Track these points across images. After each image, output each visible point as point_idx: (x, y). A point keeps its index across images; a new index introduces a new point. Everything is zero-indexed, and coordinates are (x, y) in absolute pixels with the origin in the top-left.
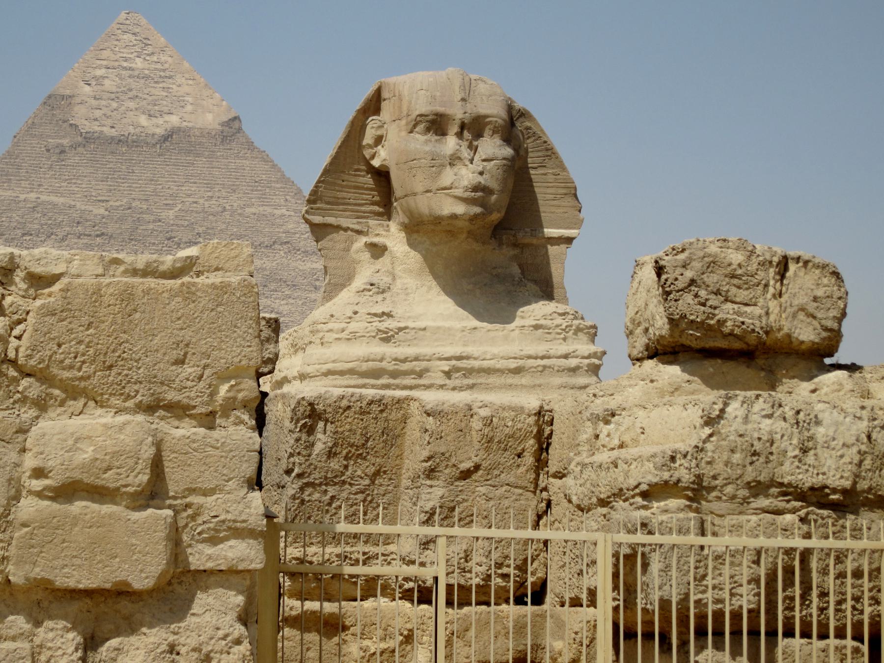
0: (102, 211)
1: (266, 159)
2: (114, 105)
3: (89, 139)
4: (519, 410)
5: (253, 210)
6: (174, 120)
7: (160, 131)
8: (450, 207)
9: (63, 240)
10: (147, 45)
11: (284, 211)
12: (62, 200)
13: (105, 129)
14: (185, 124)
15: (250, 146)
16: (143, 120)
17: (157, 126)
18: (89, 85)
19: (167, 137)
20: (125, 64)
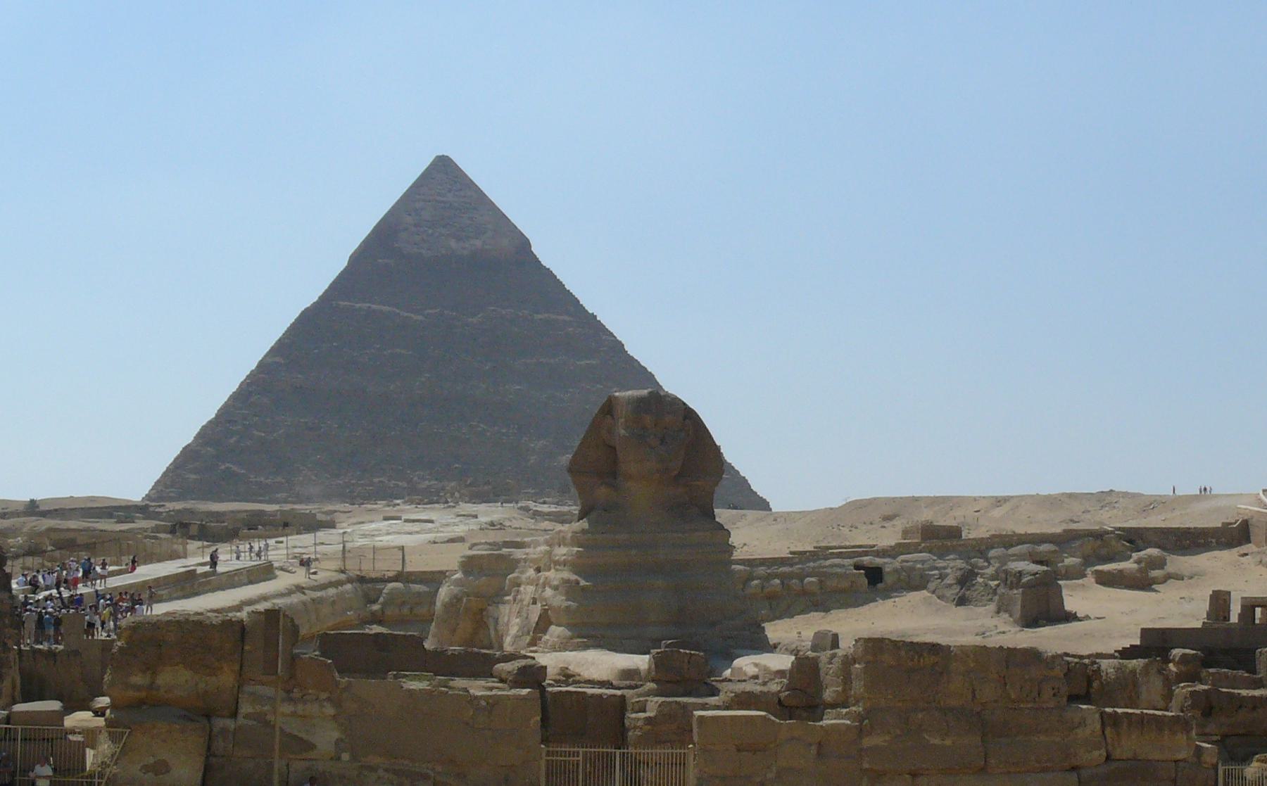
0: (420, 318)
2: (430, 231)
4: (614, 696)
5: (540, 316)
6: (478, 243)
10: (456, 182)
11: (567, 318)
12: (386, 308)
13: (423, 252)
14: (487, 247)
16: (453, 243)
18: (410, 215)
20: (439, 198)
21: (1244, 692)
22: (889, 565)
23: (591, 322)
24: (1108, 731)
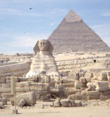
1: (85, 23)
3: (68, 23)
6: (76, 20)
7: (74, 21)
8: (42, 49)
9: (65, 33)
15: (84, 22)
17: (74, 21)
19: (75, 22)
21: (68, 80)
22: (97, 59)
23: (90, 29)
24: (30, 87)
